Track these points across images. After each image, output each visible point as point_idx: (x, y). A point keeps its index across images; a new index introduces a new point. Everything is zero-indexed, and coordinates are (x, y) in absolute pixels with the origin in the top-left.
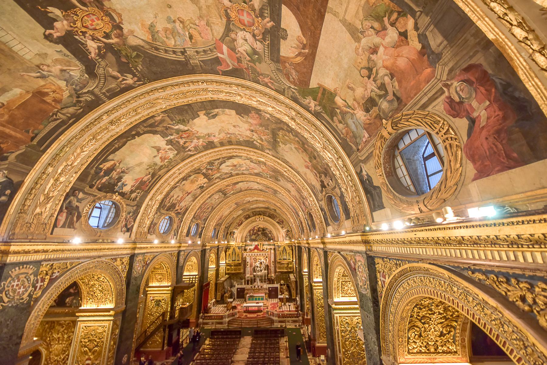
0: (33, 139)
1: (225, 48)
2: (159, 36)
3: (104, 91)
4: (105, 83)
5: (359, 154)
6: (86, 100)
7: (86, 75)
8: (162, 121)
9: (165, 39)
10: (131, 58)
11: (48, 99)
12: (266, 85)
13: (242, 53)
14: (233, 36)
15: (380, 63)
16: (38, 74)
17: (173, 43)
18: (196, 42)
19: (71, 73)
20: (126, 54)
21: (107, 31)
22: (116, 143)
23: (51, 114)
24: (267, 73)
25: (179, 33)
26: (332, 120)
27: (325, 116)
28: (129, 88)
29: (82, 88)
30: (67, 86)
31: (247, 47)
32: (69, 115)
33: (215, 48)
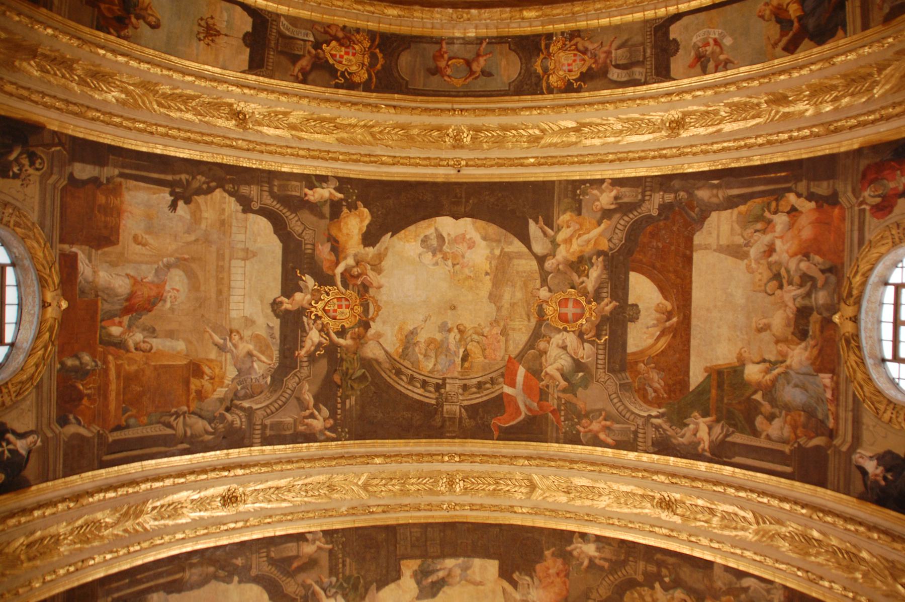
0: (119, 428)
1: (521, 372)
2: (414, 350)
3: (268, 422)
4: (281, 407)
5: (837, 442)
6: (233, 421)
7: (269, 380)
8: (311, 563)
9: (421, 357)
10: (350, 378)
11: (195, 384)
12: (596, 442)
13: (552, 377)
14: (542, 345)
15: (785, 257)
16: (221, 341)
17: (431, 366)
18: (471, 367)
19: (255, 365)
20: (347, 369)
21: (347, 326)
22: (192, 566)
23: (173, 410)
24: (599, 406)
25: (448, 349)
26: (755, 433)
27: (739, 438)
28: (309, 437)
29: (246, 397)
30: (233, 380)
31: (565, 362)
32: (189, 433)
33: (502, 375)
